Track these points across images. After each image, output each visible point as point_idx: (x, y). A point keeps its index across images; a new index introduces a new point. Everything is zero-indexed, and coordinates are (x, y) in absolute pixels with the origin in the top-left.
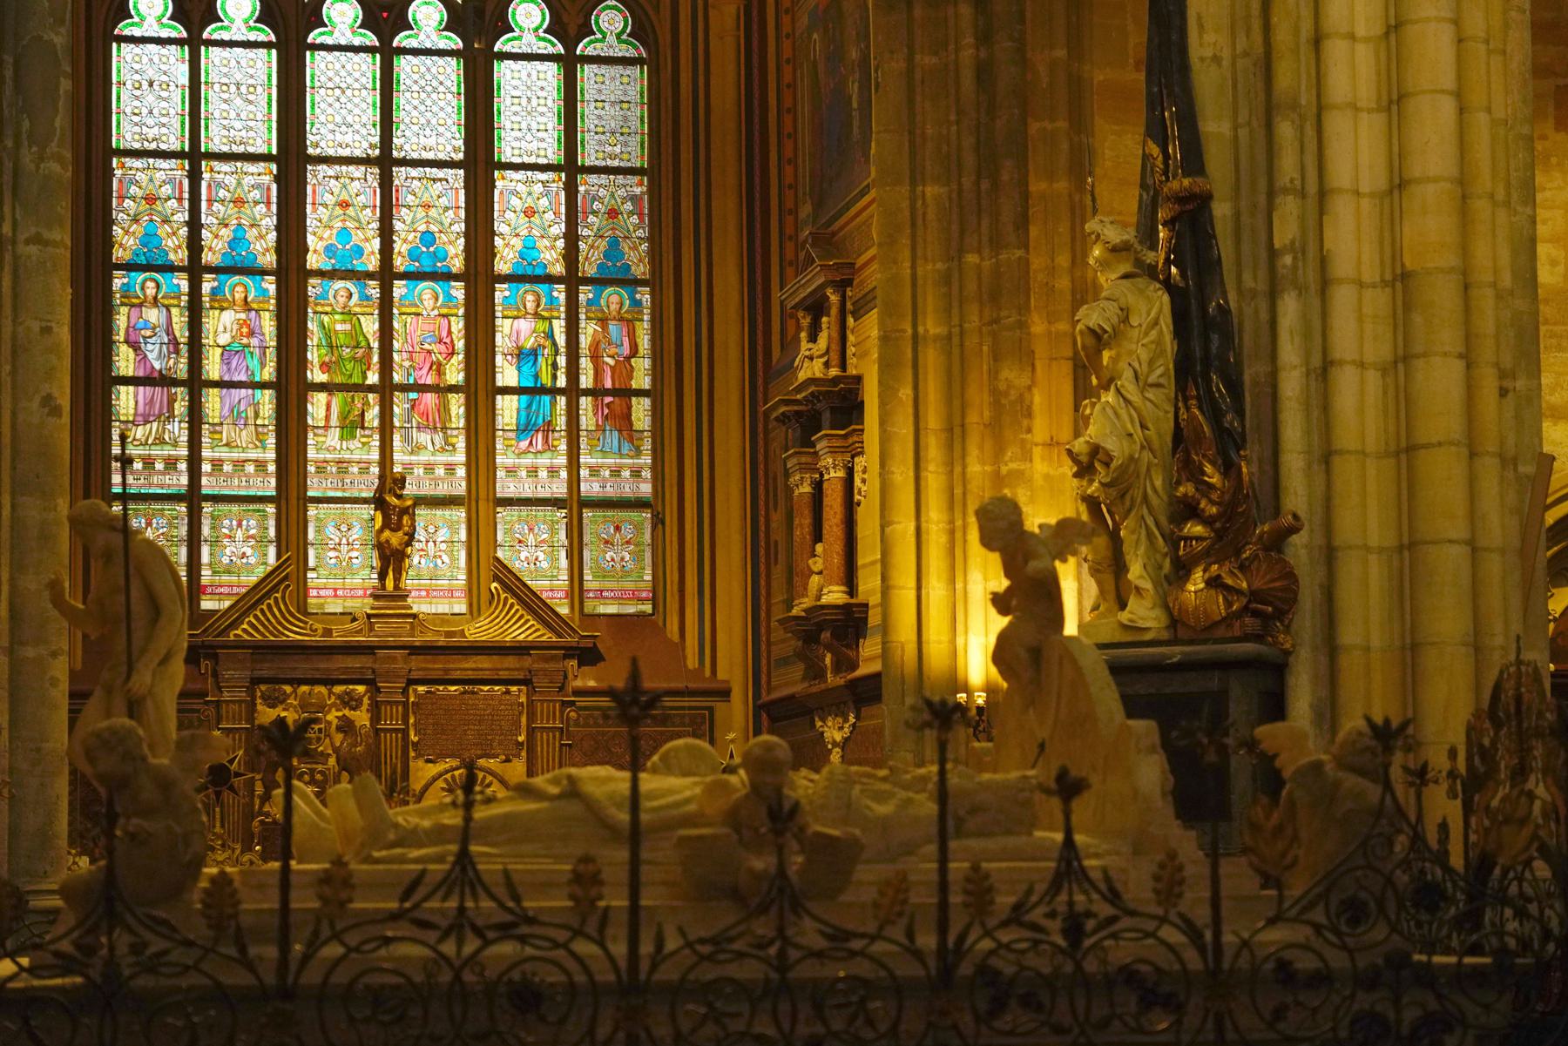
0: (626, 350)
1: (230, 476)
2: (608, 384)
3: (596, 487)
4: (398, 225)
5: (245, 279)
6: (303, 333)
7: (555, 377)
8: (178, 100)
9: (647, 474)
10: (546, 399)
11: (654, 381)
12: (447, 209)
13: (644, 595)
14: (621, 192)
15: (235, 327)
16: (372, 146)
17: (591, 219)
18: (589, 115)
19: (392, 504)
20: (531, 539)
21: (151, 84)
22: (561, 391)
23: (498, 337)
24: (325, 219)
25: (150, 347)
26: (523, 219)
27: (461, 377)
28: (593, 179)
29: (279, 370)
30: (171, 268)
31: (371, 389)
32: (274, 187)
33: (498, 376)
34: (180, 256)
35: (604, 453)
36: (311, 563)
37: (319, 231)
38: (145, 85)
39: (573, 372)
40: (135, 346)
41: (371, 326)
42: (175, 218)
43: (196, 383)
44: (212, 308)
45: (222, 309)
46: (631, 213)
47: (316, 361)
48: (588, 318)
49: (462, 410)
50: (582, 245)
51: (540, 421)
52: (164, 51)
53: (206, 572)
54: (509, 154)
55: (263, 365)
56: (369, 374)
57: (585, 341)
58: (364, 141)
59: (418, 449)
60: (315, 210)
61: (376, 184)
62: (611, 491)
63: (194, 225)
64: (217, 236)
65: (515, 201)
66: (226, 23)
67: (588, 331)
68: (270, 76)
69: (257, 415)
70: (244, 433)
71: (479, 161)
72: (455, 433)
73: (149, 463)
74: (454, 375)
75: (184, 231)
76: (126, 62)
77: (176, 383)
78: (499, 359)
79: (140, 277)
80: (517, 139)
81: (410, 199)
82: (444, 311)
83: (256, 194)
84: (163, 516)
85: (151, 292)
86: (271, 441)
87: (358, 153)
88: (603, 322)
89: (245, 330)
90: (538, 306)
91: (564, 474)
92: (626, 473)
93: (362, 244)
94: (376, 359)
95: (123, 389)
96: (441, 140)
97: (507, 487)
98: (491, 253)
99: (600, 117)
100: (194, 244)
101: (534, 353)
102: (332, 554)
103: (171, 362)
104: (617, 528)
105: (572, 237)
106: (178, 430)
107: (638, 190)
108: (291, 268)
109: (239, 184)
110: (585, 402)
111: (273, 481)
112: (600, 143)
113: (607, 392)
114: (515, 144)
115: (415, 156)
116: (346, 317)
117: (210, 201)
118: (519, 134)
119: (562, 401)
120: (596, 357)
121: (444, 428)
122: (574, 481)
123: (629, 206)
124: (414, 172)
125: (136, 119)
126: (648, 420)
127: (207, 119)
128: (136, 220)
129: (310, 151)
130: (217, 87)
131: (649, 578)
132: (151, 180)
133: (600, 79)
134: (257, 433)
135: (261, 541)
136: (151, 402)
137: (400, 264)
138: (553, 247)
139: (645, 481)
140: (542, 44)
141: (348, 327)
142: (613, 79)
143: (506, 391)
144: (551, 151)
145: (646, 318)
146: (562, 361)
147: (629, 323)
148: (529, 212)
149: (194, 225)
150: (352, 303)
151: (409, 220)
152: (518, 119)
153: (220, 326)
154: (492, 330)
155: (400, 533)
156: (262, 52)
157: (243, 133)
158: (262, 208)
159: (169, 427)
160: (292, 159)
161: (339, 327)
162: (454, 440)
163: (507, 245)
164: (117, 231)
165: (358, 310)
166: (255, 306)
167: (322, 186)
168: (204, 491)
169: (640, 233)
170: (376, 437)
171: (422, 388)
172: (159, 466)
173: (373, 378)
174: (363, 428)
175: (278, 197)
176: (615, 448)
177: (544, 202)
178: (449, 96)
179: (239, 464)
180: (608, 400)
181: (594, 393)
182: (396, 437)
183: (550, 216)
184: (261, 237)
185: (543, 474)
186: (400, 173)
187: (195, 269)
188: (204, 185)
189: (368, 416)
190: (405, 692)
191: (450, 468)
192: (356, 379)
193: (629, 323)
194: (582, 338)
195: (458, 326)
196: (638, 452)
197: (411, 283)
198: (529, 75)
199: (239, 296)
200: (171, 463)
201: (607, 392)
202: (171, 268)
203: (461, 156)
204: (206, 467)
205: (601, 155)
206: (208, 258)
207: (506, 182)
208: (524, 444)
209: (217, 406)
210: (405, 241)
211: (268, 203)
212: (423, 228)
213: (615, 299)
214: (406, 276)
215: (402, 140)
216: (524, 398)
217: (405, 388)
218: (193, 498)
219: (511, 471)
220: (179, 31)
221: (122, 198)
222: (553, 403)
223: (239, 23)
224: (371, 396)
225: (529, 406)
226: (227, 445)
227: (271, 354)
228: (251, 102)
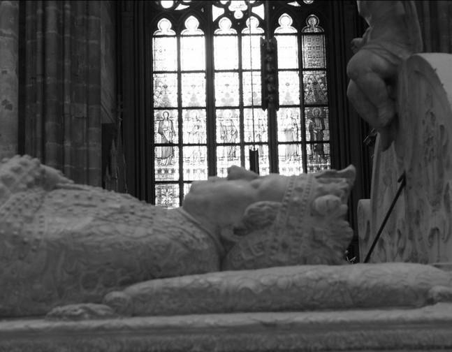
0: (321, 128)
7: (297, 137)
14: (318, 76)
31: (238, 144)
34: (175, 104)
39: (304, 135)
40: (162, 134)
46: (321, 83)
73: (166, 171)
76: (157, 44)
77: (175, 145)
79: (163, 111)
85: (166, 116)
88: (313, 119)
95: (157, 147)
101: (291, 130)
107: (323, 75)
108: (211, 108)
110: (308, 146)
113: (315, 142)
120: (311, 131)
123: (320, 81)
128: (161, 93)
136: (166, 152)
137: (246, 104)
146: (300, 132)
147: (322, 119)
164: (155, 97)
169: (324, 89)
173: (238, 141)
180: (315, 144)
181: (311, 142)
201: (315, 142)
217: (249, 144)
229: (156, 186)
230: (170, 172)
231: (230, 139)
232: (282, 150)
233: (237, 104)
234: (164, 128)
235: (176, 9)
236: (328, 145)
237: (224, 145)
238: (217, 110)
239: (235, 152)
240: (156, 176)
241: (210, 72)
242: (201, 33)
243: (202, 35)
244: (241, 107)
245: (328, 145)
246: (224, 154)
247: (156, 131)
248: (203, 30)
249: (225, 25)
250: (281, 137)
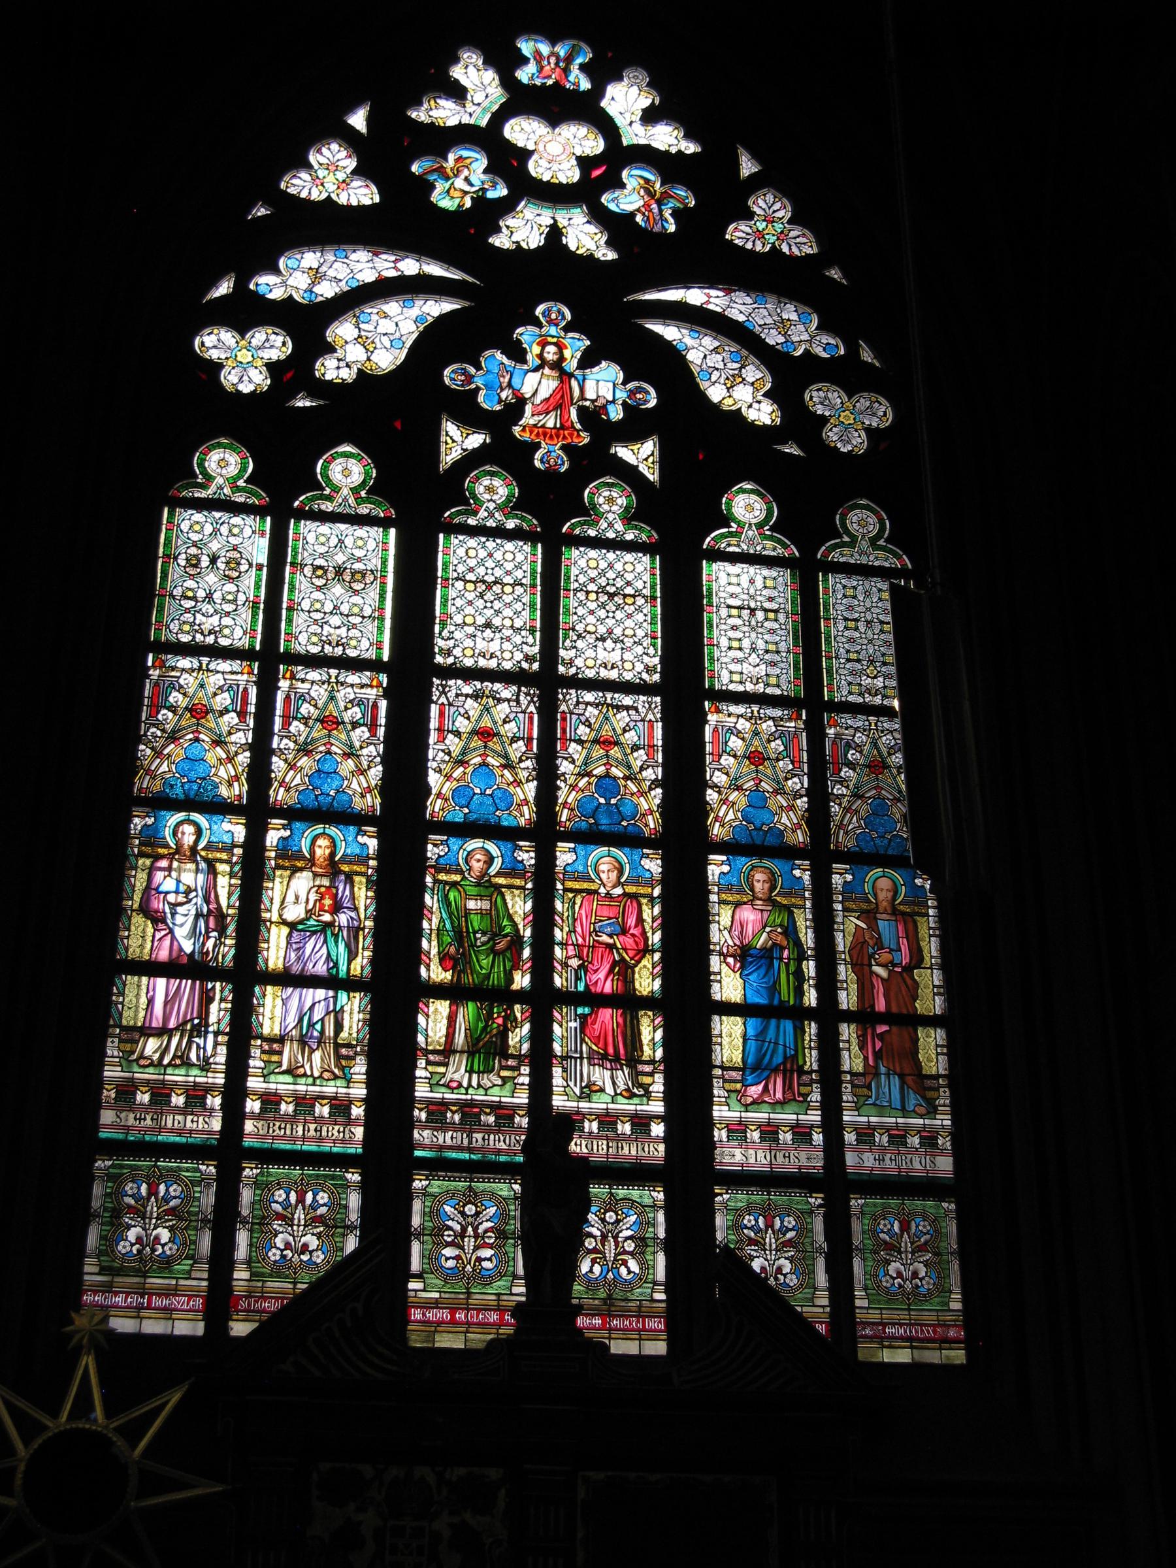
0: (904, 957)
1: (292, 1119)
2: (881, 1005)
3: (869, 1160)
4: (565, 767)
5: (333, 831)
6: (418, 911)
7: (799, 992)
8: (251, 585)
9: (944, 1142)
10: (788, 1025)
11: (950, 1000)
12: (635, 748)
13: (952, 1333)
15: (313, 897)
16: (527, 658)
17: (845, 772)
18: (837, 635)
20: (770, 1238)
21: (214, 560)
22: (810, 1014)
23: (714, 927)
24: (456, 750)
25: (179, 919)
26: (747, 767)
27: (657, 984)
28: (847, 719)
29: (373, 961)
30: (218, 808)
31: (521, 996)
32: (383, 705)
33: (715, 987)
34: (240, 790)
35: (881, 1110)
36: (415, 1264)
37: (446, 768)
38: (205, 561)
39: (827, 984)
41: (520, 906)
42: (233, 738)
43: (247, 976)
44: (278, 867)
45: (295, 870)
47: (434, 951)
48: (845, 910)
49: (659, 1034)
50: (835, 808)
51: (779, 1059)
52: (237, 520)
53: (241, 1274)
54: (725, 680)
55: (351, 958)
56: (517, 976)
57: (842, 942)
58: (515, 649)
59: (589, 1090)
60: (442, 739)
61: (532, 708)
62: (890, 1165)
63: (261, 750)
64: (292, 766)
65: (735, 743)
66: (327, 491)
67: (847, 930)
68: (384, 562)
69: (339, 1027)
70: (317, 1055)
71: (683, 686)
72: (648, 1068)
74: (647, 982)
75: (244, 758)
78: (715, 962)
80: (737, 661)
81: (583, 731)
82: (631, 889)
83: (356, 713)
84: (178, 1180)
86: (360, 1068)
87: (507, 665)
88: (870, 915)
89: (328, 902)
90: (773, 888)
91: (818, 1138)
93: (511, 789)
94: (527, 953)
95: (131, 980)
96: (628, 656)
97: (732, 1156)
98: (703, 809)
99: (851, 640)
100: (259, 774)
101: (768, 955)
102: (448, 1252)
103: (210, 944)
104: (905, 1227)
105: (818, 795)
108: (403, 814)
109: (332, 698)
110: (847, 1031)
111: (359, 1132)
112: (853, 672)
114: (733, 667)
115: (590, 674)
116: (483, 892)
117: (287, 719)
118: (739, 654)
119: (812, 1029)
120: (861, 966)
122: (834, 1147)
124: (589, 697)
125: (189, 604)
127: (290, 609)
129: (439, 659)
130: (308, 571)
131: (956, 1306)
132: (202, 686)
133: (850, 592)
134: (338, 1057)
135: (330, 1224)
138: (791, 808)
139: (942, 1152)
140: (769, 544)
141: (486, 905)
142: (867, 594)
144: (784, 679)
145: (931, 912)
146: (810, 968)
148: (756, 758)
149: (261, 750)
150: (493, 870)
151: (579, 757)
152: (738, 635)
153: (290, 895)
154: (703, 919)
156: (375, 532)
157: (343, 632)
158: (362, 733)
159: (201, 1041)
160: (412, 669)
161: (471, 904)
162: (646, 1080)
163: (724, 801)
164: (144, 750)
165: (501, 881)
166: (345, 868)
167: (454, 711)
168: (247, 1142)
170: (525, 1070)
172: (178, 1100)
173: (521, 980)
175: (388, 716)
177: (777, 745)
178: (640, 601)
179: (304, 1103)
180: (881, 1029)
181: (864, 1017)
182: (557, 1071)
183: (785, 765)
184: (363, 772)
185: (786, 1137)
186: (569, 699)
187: (257, 810)
188: (280, 697)
189: (514, 1039)
191: (641, 1122)
193: (907, 918)
194: (839, 937)
195: (650, 913)
196: (932, 1111)
197: (581, 849)
198: (752, 581)
199: (322, 850)
200: (196, 1096)
203: (656, 677)
204: (253, 1105)
205: (855, 689)
206: (278, 795)
207: (721, 717)
208: (755, 1091)
209: (278, 1011)
210: (573, 787)
211: (373, 727)
212: (600, 771)
213: (884, 884)
214: (569, 836)
215: (572, 653)
216: (752, 1022)
217: (571, 998)
218: (228, 1151)
219: (738, 1130)
220: (260, 498)
221: (156, 708)
222: (800, 1031)
223: (345, 491)
224: (517, 1007)
226: (288, 1072)
227: (365, 942)
228: (356, 592)
236: (940, 1035)
237: (454, 993)
240: (107, 1116)
245: (940, 1035)
249: (493, 491)
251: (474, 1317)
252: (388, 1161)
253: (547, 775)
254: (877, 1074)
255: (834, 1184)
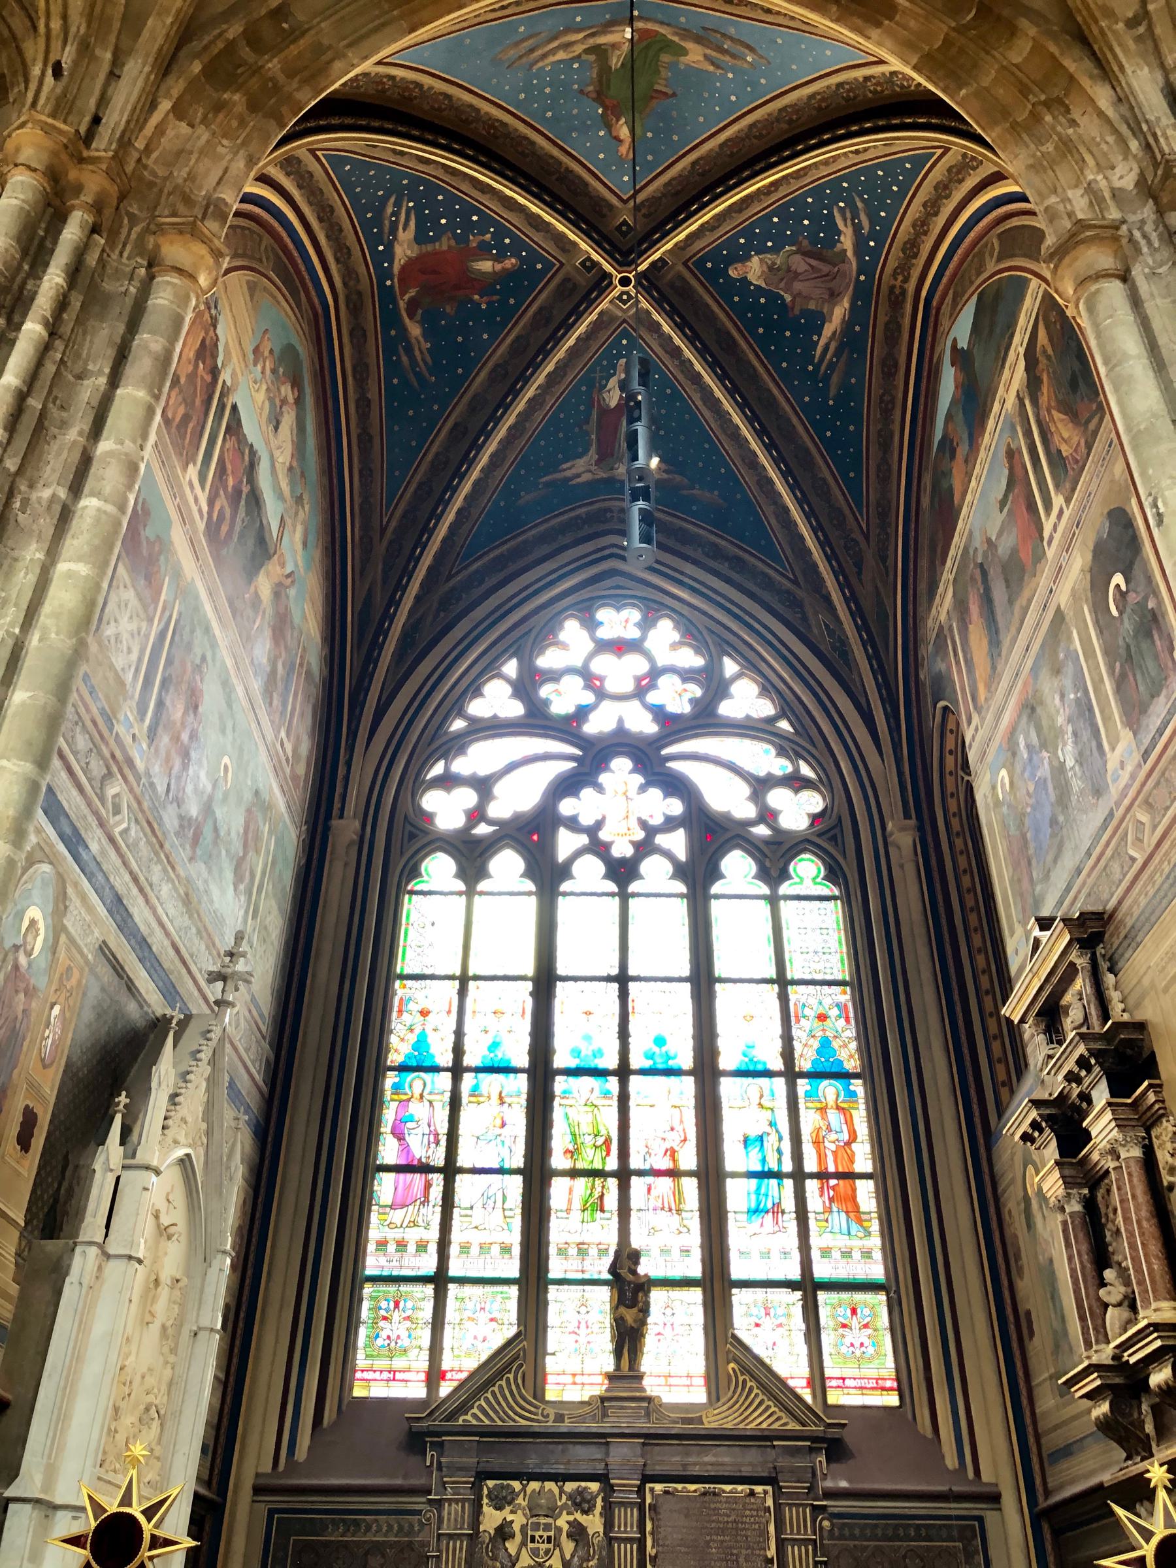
7: (780, 1161)
19: (629, 1288)
31: (612, 1174)
51: (770, 1205)
67: (809, 1121)
74: (688, 1159)
88: (823, 1110)
92: (856, 1255)
101: (761, 1138)
106: (434, 1215)
110: (812, 1186)
120: (818, 1143)
121: (679, 1211)
126: (874, 1203)
139: (876, 1262)
143: (734, 1175)
155: (635, 1310)
171: (658, 1173)
173: (612, 1164)
174: (602, 1210)
176: (845, 1230)
180: (833, 1182)
190: (641, 1491)
192: (598, 1165)
202: (436, 1069)
225: (758, 1188)
229: (368, 1289)
230: (411, 1248)
231: (590, 1159)
232: (738, 1194)
233: (612, 1063)
234: (410, 1117)
235: (474, 831)
237: (574, 1173)
238: (558, 1078)
239: (601, 1197)
241: (545, 982)
242: (530, 886)
243: (529, 894)
244: (623, 1072)
246: (570, 1201)
247: (386, 1128)
248: (534, 881)
250: (734, 1157)
251: (586, 1379)
252: (533, 1281)
253: (624, 1034)
254: (831, 1212)
255: (809, 1287)
